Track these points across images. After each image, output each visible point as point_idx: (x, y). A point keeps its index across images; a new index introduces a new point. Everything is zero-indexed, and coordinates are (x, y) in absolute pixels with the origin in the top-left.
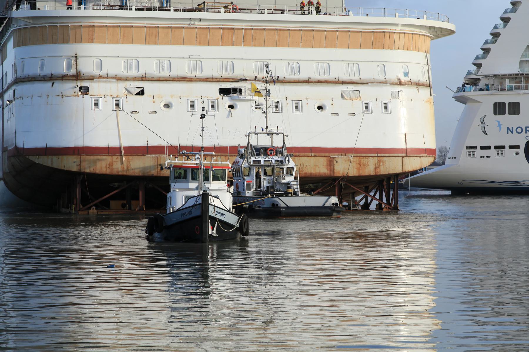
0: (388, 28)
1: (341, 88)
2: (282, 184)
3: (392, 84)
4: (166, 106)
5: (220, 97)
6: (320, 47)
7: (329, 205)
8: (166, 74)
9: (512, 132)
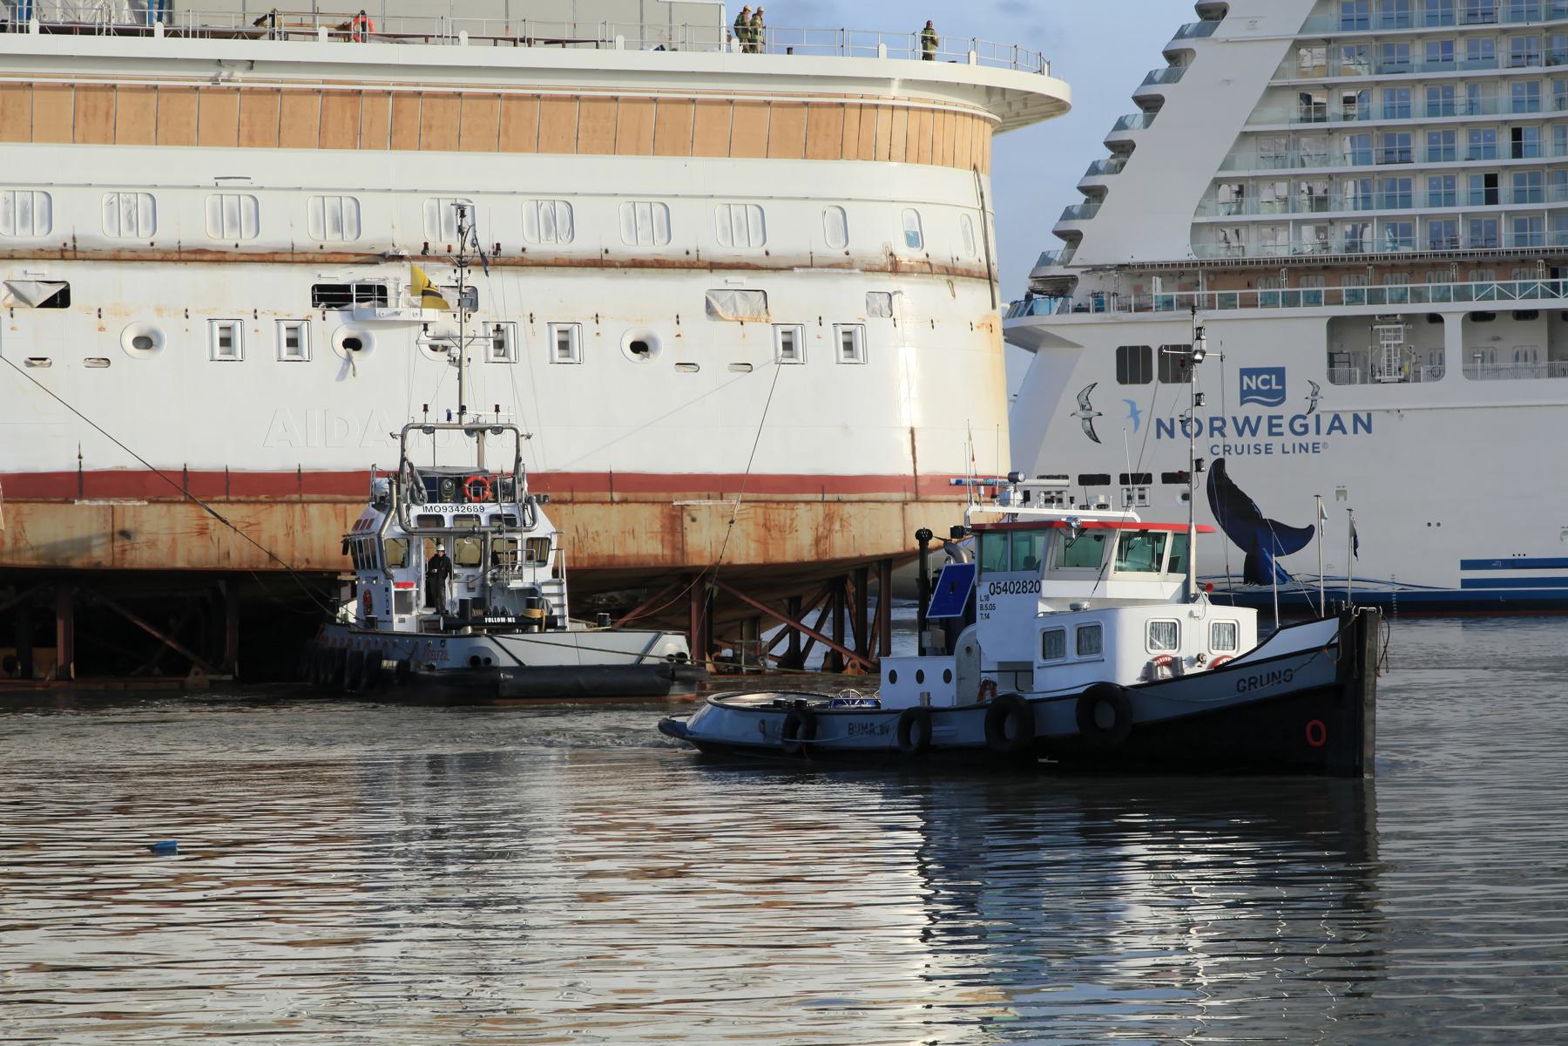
0: (854, 94)
1: (707, 282)
3: (870, 270)
5: (317, 312)
6: (638, 152)
8: (140, 238)
9: (1171, 434)
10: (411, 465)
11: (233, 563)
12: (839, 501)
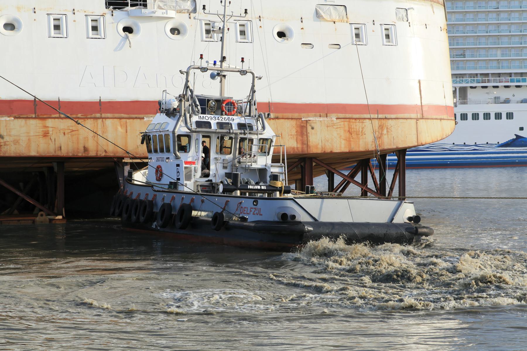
2: (254, 170)
4: (10, 27)
5: (108, 12)
7: (402, 222)
10: (191, 91)
11: (64, 152)
12: (386, 118)
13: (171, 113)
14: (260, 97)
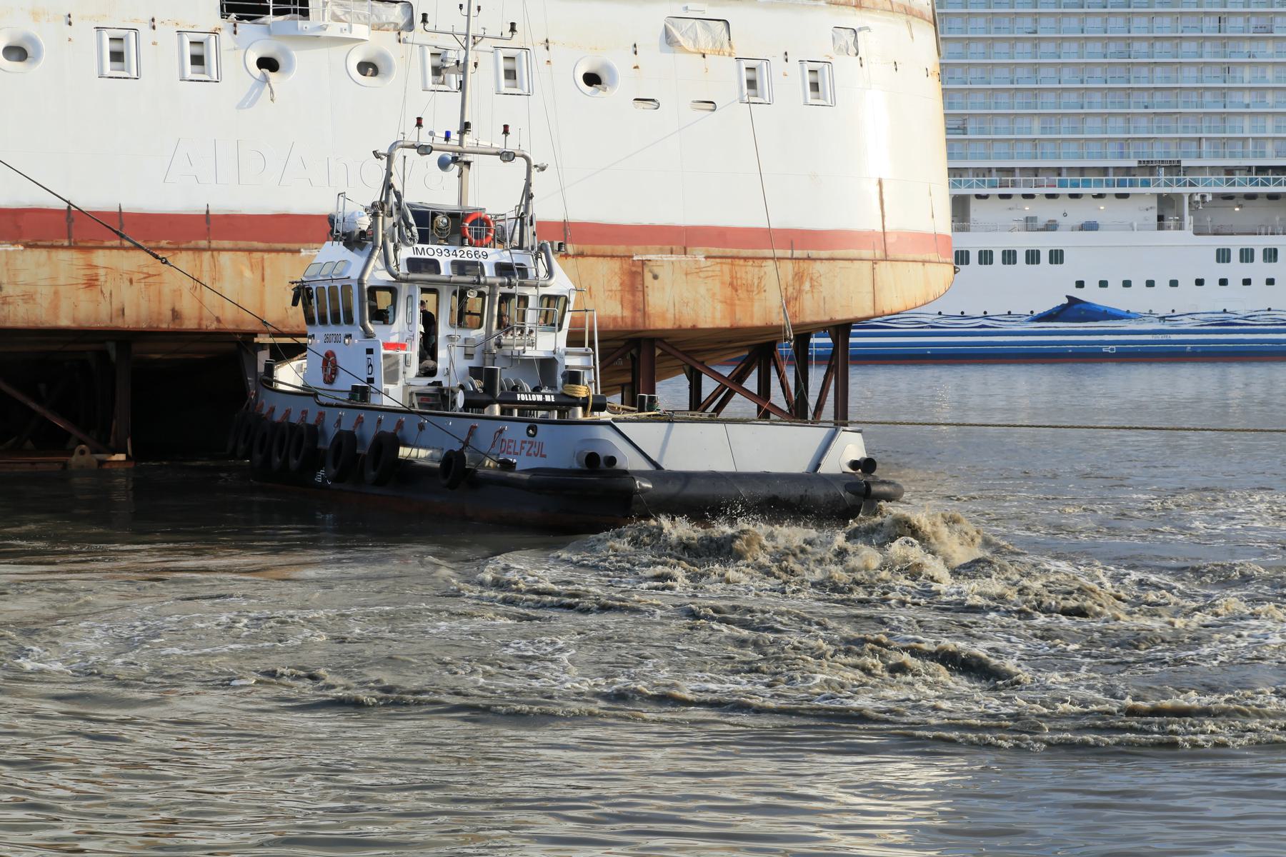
2: (530, 362)
4: (16, 55)
5: (225, 25)
10: (398, 195)
12: (809, 258)
13: (356, 241)
14: (543, 210)
